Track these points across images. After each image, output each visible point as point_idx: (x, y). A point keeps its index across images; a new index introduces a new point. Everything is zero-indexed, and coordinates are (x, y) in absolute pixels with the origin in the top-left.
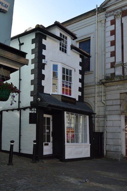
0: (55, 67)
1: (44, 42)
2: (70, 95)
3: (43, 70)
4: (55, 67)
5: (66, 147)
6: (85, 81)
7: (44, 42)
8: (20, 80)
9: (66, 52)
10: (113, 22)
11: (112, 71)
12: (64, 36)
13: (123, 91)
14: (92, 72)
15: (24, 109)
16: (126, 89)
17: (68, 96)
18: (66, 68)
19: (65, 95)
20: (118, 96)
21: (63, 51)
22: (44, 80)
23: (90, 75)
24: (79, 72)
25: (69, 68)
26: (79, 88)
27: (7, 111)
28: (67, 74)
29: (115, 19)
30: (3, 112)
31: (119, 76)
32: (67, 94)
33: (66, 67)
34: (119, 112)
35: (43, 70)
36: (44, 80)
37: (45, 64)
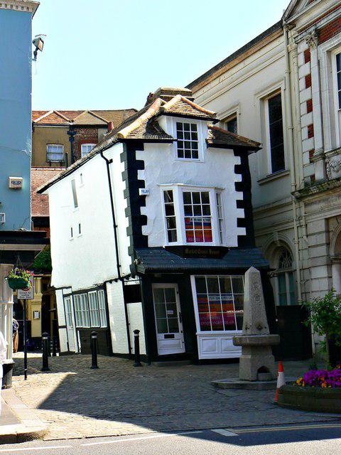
0: (169, 196)
1: (139, 155)
2: (210, 239)
3: (142, 208)
4: (169, 196)
5: (199, 340)
6: (255, 201)
7: (139, 155)
8: (115, 226)
9: (196, 155)
10: (307, 59)
11: (309, 171)
12: (187, 127)
13: (329, 215)
14: (288, 173)
15: (127, 277)
16: (339, 208)
18: (191, 191)
19: (195, 244)
20: (321, 226)
21: (188, 156)
23: (275, 183)
24: (233, 187)
25: (200, 190)
26: (239, 219)
27: (111, 282)
28: (196, 200)
29: (309, 49)
30: (108, 285)
31: (320, 183)
33: (191, 190)
34: (324, 260)
35: (142, 208)
37: (144, 197)
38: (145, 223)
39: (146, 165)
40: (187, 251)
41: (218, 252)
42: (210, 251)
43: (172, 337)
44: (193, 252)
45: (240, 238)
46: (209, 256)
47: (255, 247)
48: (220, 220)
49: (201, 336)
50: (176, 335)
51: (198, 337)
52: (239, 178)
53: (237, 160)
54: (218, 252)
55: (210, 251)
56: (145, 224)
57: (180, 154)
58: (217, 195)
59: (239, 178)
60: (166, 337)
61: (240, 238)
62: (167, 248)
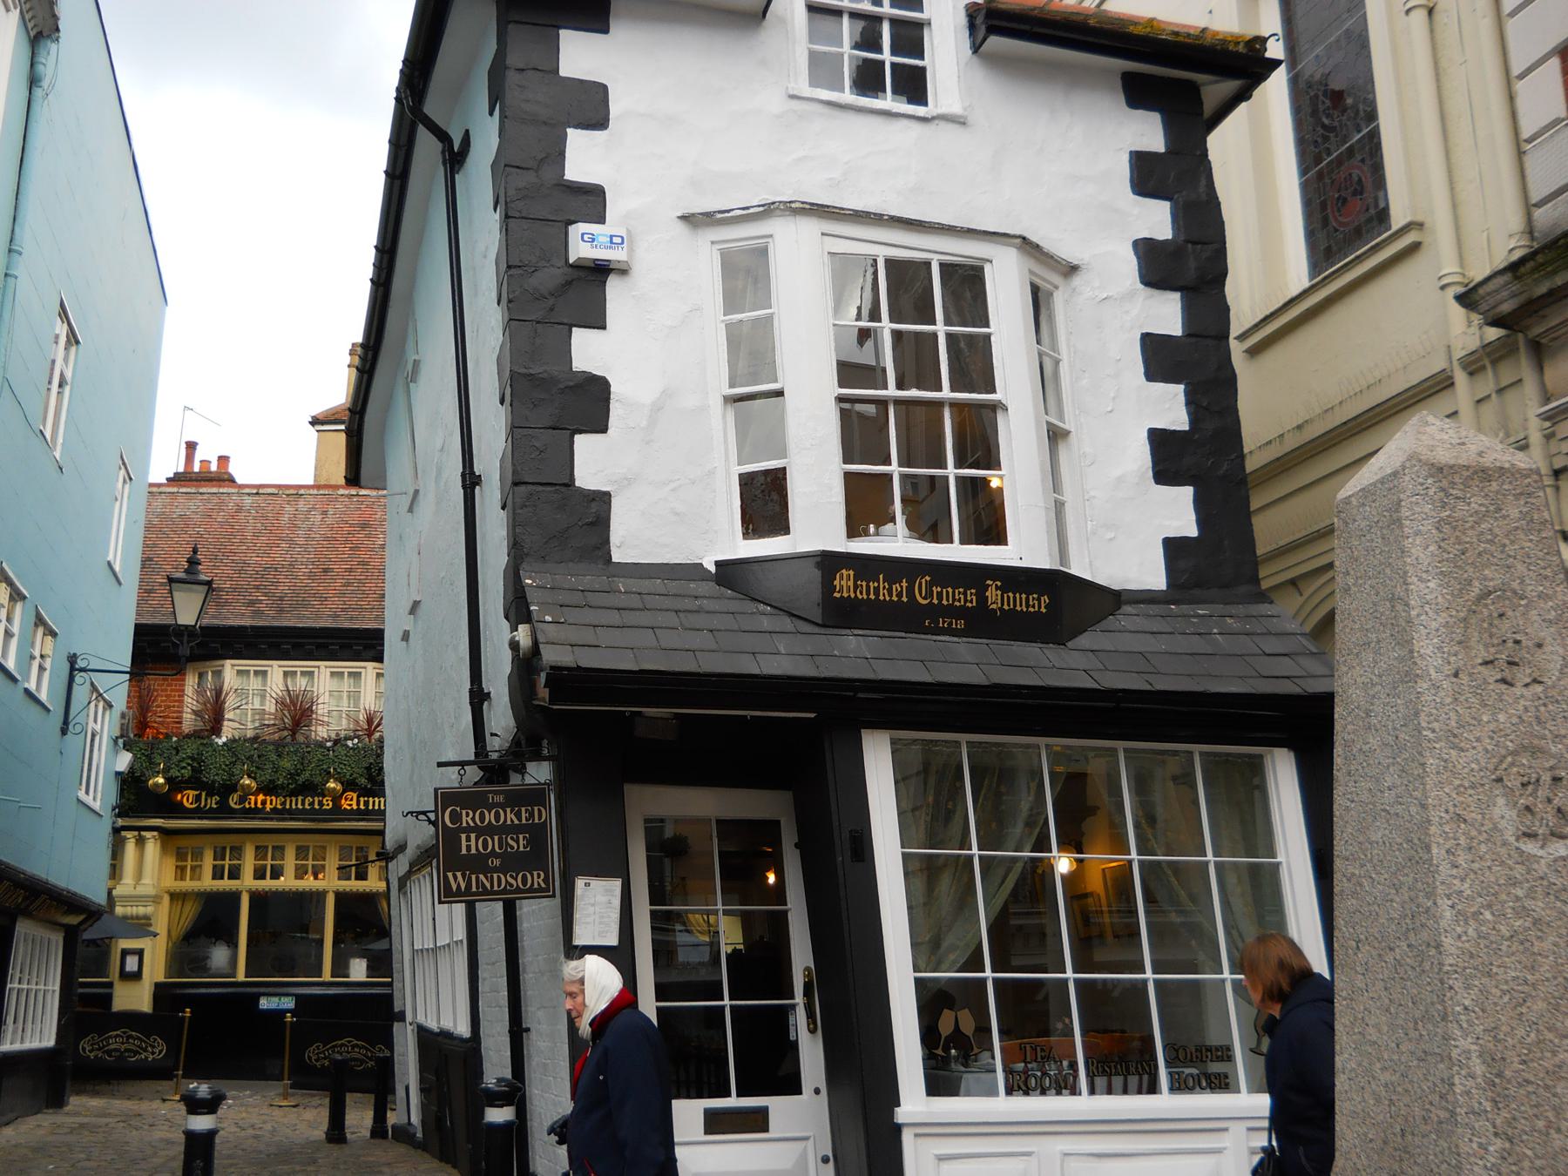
2: (990, 527)
9: (913, 85)
17: (956, 552)
18: (882, 253)
21: (868, 79)
22: (601, 427)
24: (1129, 265)
25: (935, 250)
32: (934, 531)
36: (601, 427)
37: (600, 272)
38: (599, 425)
39: (617, 106)
40: (845, 582)
41: (1039, 604)
42: (993, 594)
43: (756, 1122)
44: (883, 591)
45: (1174, 548)
46: (982, 623)
47: (1263, 597)
48: (1056, 436)
49: (931, 1129)
50: (777, 1105)
51: (907, 1137)
52: (1157, 220)
53: (1149, 132)
54: (1039, 604)
55: (993, 594)
56: (599, 425)
57: (823, 71)
58: (1039, 300)
59: (1157, 220)
60: (716, 1123)
61: (1174, 548)
62: (730, 573)
